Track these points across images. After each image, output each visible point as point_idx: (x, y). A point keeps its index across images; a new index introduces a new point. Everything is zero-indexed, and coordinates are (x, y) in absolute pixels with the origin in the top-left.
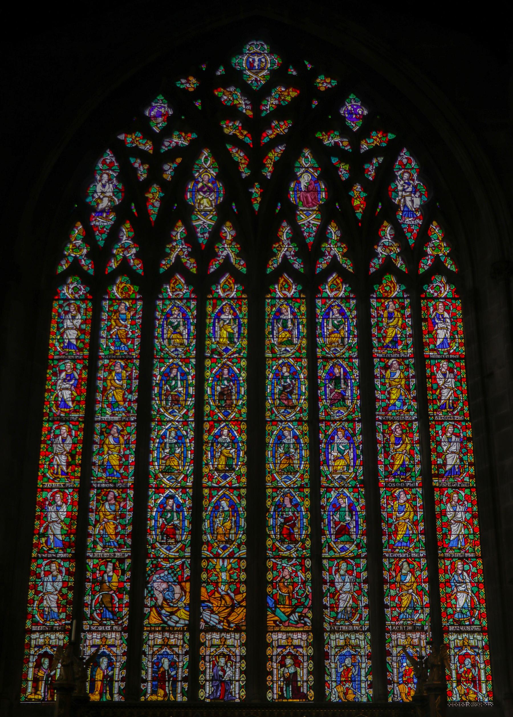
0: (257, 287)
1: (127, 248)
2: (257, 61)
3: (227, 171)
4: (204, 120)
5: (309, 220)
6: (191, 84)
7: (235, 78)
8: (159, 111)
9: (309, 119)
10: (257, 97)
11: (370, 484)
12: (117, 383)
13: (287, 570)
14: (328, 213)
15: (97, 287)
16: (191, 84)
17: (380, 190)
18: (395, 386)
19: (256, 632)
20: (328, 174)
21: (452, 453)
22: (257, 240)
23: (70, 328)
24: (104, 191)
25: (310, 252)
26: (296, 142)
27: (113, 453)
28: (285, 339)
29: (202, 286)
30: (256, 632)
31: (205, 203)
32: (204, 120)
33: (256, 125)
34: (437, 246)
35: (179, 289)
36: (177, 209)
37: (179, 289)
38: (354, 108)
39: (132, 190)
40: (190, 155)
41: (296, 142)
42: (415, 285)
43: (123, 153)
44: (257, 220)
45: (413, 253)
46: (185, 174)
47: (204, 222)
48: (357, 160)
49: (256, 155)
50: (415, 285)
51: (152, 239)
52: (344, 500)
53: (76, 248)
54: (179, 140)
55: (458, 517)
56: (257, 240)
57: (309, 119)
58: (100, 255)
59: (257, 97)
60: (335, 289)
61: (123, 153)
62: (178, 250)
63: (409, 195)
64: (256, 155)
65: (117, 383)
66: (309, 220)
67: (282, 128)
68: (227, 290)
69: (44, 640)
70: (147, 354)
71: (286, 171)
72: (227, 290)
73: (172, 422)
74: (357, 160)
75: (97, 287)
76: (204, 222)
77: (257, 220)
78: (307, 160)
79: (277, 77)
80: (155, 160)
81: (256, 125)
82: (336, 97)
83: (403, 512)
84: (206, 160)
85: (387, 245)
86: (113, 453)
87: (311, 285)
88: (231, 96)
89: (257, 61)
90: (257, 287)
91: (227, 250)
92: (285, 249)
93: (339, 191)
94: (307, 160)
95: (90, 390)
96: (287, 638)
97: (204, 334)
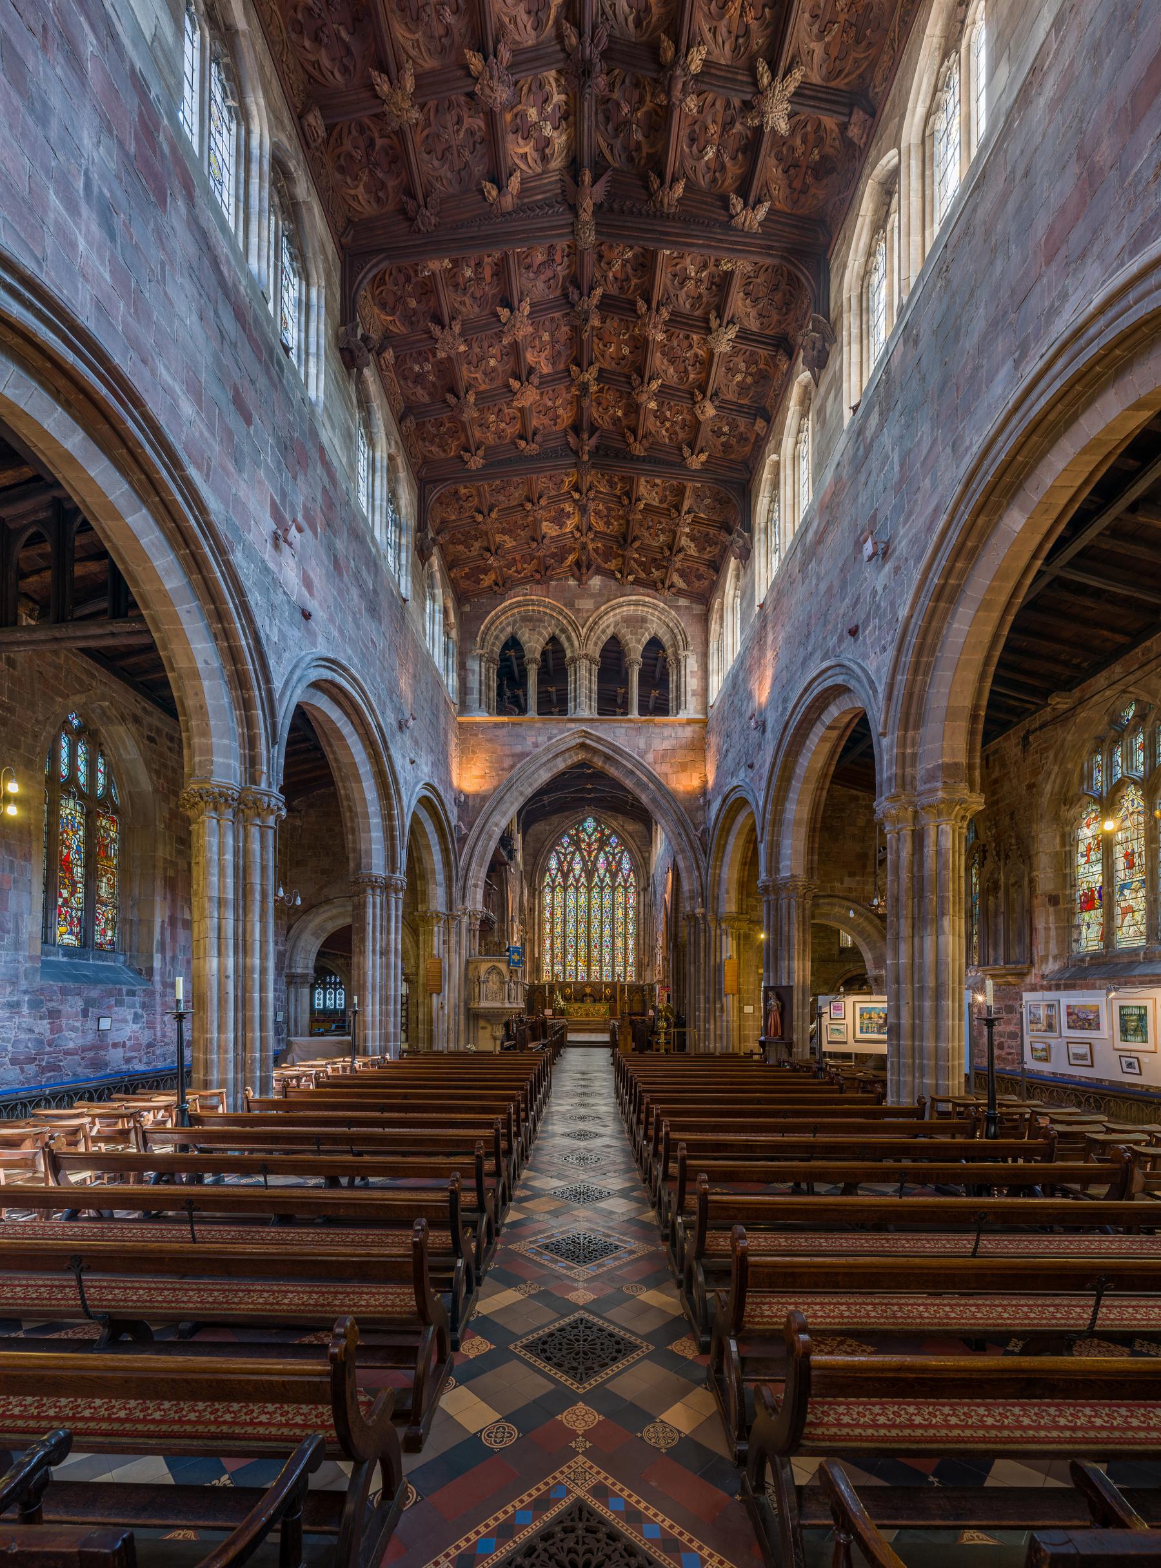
0: (589, 890)
1: (559, 879)
2: (590, 824)
3: (583, 858)
4: (576, 843)
5: (602, 871)
6: (573, 832)
7: (584, 830)
8: (565, 840)
9: (603, 843)
10: (590, 836)
11: (613, 936)
12: (559, 912)
13: (595, 954)
14: (607, 870)
15: (553, 889)
16: (573, 832)
17: (619, 863)
18: (620, 913)
19: (589, 966)
20: (607, 859)
21: (631, 929)
22: (590, 877)
23: (548, 898)
24: (553, 864)
25: (602, 881)
26: (600, 849)
27: (559, 929)
28: (595, 903)
29: (577, 889)
30: (589, 966)
31: (577, 867)
32: (576, 843)
33: (589, 845)
34: (632, 879)
35: (571, 890)
36: (571, 869)
37: (571, 890)
38: (614, 839)
39: (560, 863)
40: (573, 853)
41: (600, 849)
42: (626, 889)
43: (558, 853)
44: (590, 873)
45: (626, 881)
46: (572, 859)
47: (577, 872)
48: (614, 855)
49: (589, 855)
50: (626, 889)
51: (565, 876)
52: (607, 938)
53: (548, 879)
54: (570, 849)
55: (631, 943)
56: (590, 877)
57: (603, 843)
58: (553, 881)
59: (590, 836)
60: (607, 890)
61: (558, 853)
62: (571, 880)
63: (626, 865)
64: (589, 855)
65: (559, 912)
66: (602, 871)
67: (595, 846)
68: (583, 890)
69: (547, 968)
70: (565, 906)
71: (596, 858)
72: (583, 890)
73: (571, 923)
74: (614, 855)
75: (553, 889)
76: (577, 872)
77: (590, 873)
78: (602, 854)
79: (595, 830)
80: (565, 855)
81: (589, 845)
82: (609, 837)
83: (619, 942)
84: (578, 857)
85: (619, 879)
86: (559, 929)
87: (602, 889)
88: (583, 835)
89: (590, 824)
90: (589, 890)
91: (583, 880)
92: (596, 880)
93: (609, 864)
94: (602, 854)
95: (552, 914)
96: (595, 968)
97: (576, 900)
